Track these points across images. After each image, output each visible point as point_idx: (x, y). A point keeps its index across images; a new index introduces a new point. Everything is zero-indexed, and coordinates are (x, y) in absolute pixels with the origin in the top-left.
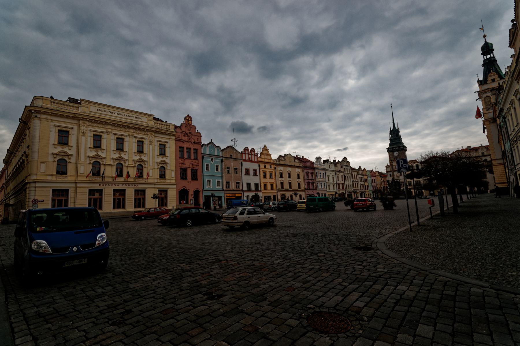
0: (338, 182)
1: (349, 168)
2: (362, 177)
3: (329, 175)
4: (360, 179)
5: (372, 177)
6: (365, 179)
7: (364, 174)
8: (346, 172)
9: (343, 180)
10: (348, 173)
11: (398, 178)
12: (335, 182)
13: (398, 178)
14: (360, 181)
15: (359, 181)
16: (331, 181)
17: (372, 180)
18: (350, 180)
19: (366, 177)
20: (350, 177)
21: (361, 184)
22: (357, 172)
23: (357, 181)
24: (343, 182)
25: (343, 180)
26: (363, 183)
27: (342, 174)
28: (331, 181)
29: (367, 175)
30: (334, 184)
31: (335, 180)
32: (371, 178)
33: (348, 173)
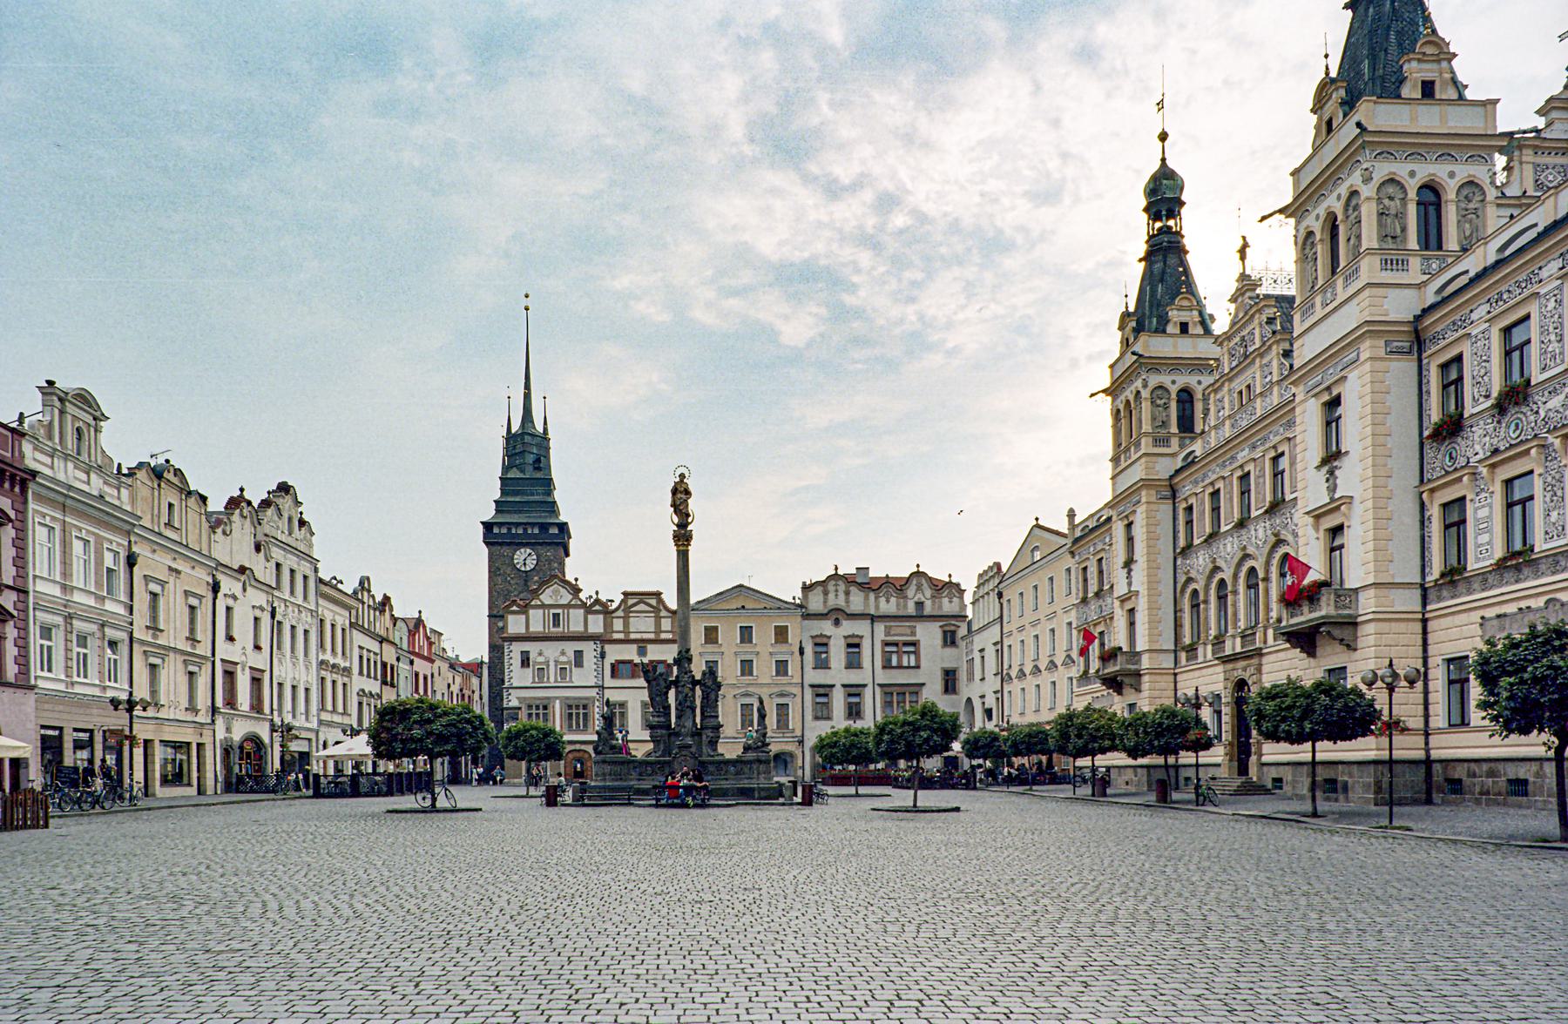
0: (224, 651)
1: (304, 568)
2: (374, 646)
3: (163, 583)
4: (361, 657)
5: (416, 660)
6: (384, 665)
7: (383, 633)
8: (287, 596)
9: (265, 644)
10: (300, 601)
11: (563, 678)
12: (204, 649)
13: (563, 678)
14: (361, 673)
15: (356, 670)
16: (174, 635)
17: (417, 675)
18: (306, 654)
19: (389, 655)
20: (306, 632)
21: (362, 693)
22: (348, 608)
23: (347, 671)
24: (261, 661)
25: (265, 644)
26: (373, 686)
27: (260, 598)
28: (174, 635)
29: (397, 641)
30: (189, 658)
31: (203, 634)
32: (412, 662)
33: (300, 601)
